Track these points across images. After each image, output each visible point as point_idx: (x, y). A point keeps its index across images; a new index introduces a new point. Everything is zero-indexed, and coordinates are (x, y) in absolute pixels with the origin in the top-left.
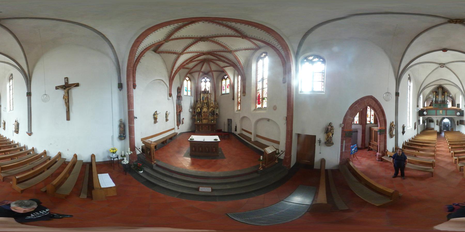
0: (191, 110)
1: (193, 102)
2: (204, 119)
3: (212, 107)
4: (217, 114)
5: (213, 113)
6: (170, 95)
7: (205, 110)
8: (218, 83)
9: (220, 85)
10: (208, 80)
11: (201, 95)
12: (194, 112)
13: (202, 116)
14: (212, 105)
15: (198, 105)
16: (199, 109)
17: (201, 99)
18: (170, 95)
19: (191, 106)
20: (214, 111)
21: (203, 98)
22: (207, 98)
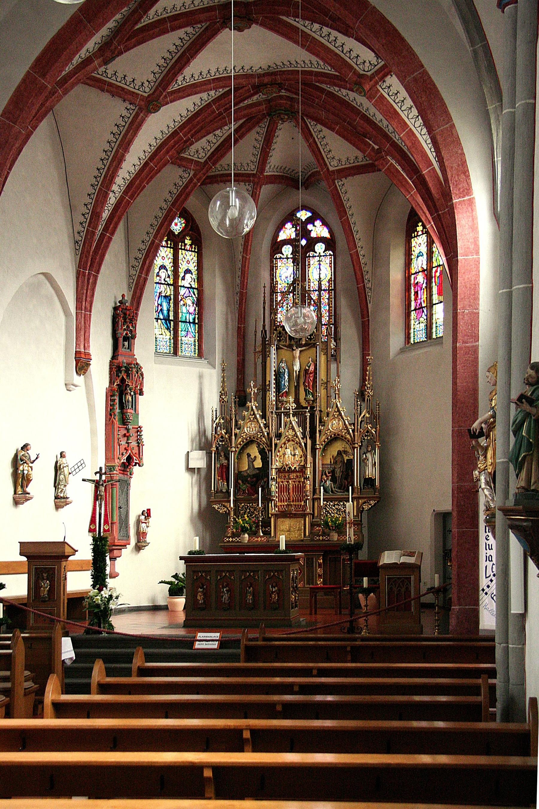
0: (198, 460)
1: (212, 402)
2: (283, 514)
3: (335, 438)
4: (369, 482)
5: (342, 476)
6: (82, 364)
7: (288, 456)
8: (380, 260)
9: (396, 275)
10: (318, 230)
11: (265, 354)
12: (224, 471)
13: (267, 498)
14: (334, 425)
15: (249, 429)
16: (254, 451)
17: (264, 389)
18: (82, 364)
19: (202, 433)
20: (350, 462)
21: (278, 375)
22: (308, 376)
